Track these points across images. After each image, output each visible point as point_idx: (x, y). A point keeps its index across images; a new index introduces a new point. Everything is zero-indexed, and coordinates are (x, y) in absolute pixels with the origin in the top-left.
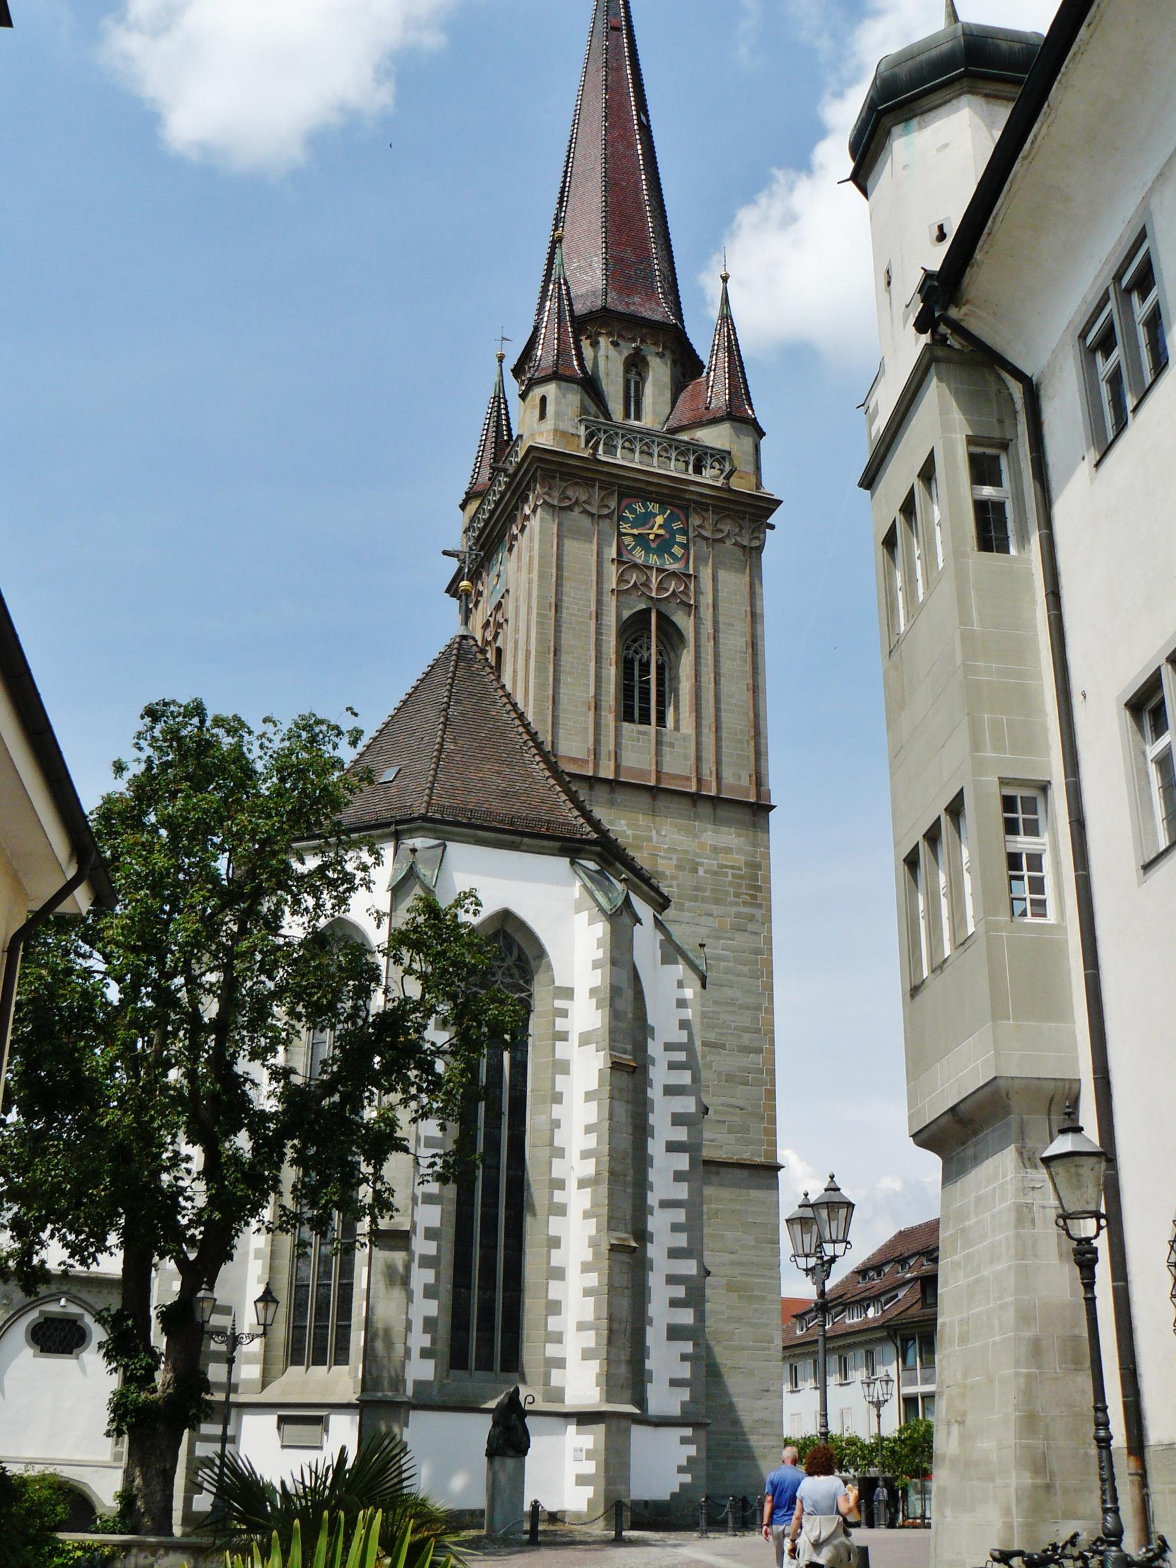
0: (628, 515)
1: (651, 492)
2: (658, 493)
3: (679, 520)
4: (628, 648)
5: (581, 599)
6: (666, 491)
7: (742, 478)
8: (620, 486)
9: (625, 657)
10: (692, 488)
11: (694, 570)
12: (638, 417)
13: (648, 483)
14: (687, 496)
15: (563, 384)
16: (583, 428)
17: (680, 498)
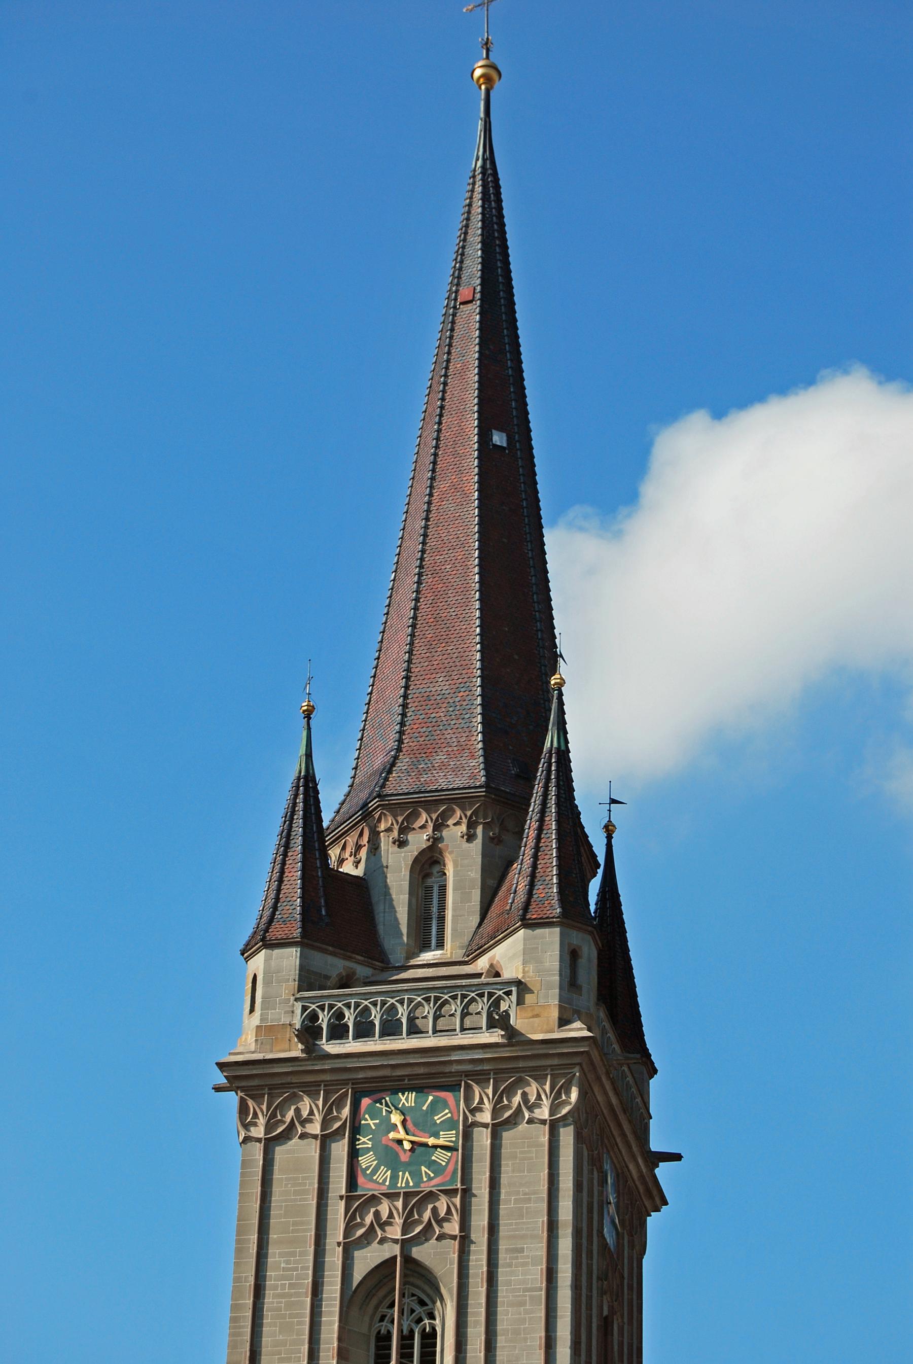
0: (371, 1122)
1: (401, 1078)
2: (411, 1077)
3: (446, 1105)
4: (382, 1319)
5: (296, 1269)
6: (422, 1070)
7: (537, 1016)
8: (355, 1082)
9: (379, 1332)
10: (455, 1057)
11: (462, 1183)
12: (440, 945)
13: (393, 1067)
14: (455, 1068)
15: (277, 952)
16: (298, 1011)
17: (444, 1074)
